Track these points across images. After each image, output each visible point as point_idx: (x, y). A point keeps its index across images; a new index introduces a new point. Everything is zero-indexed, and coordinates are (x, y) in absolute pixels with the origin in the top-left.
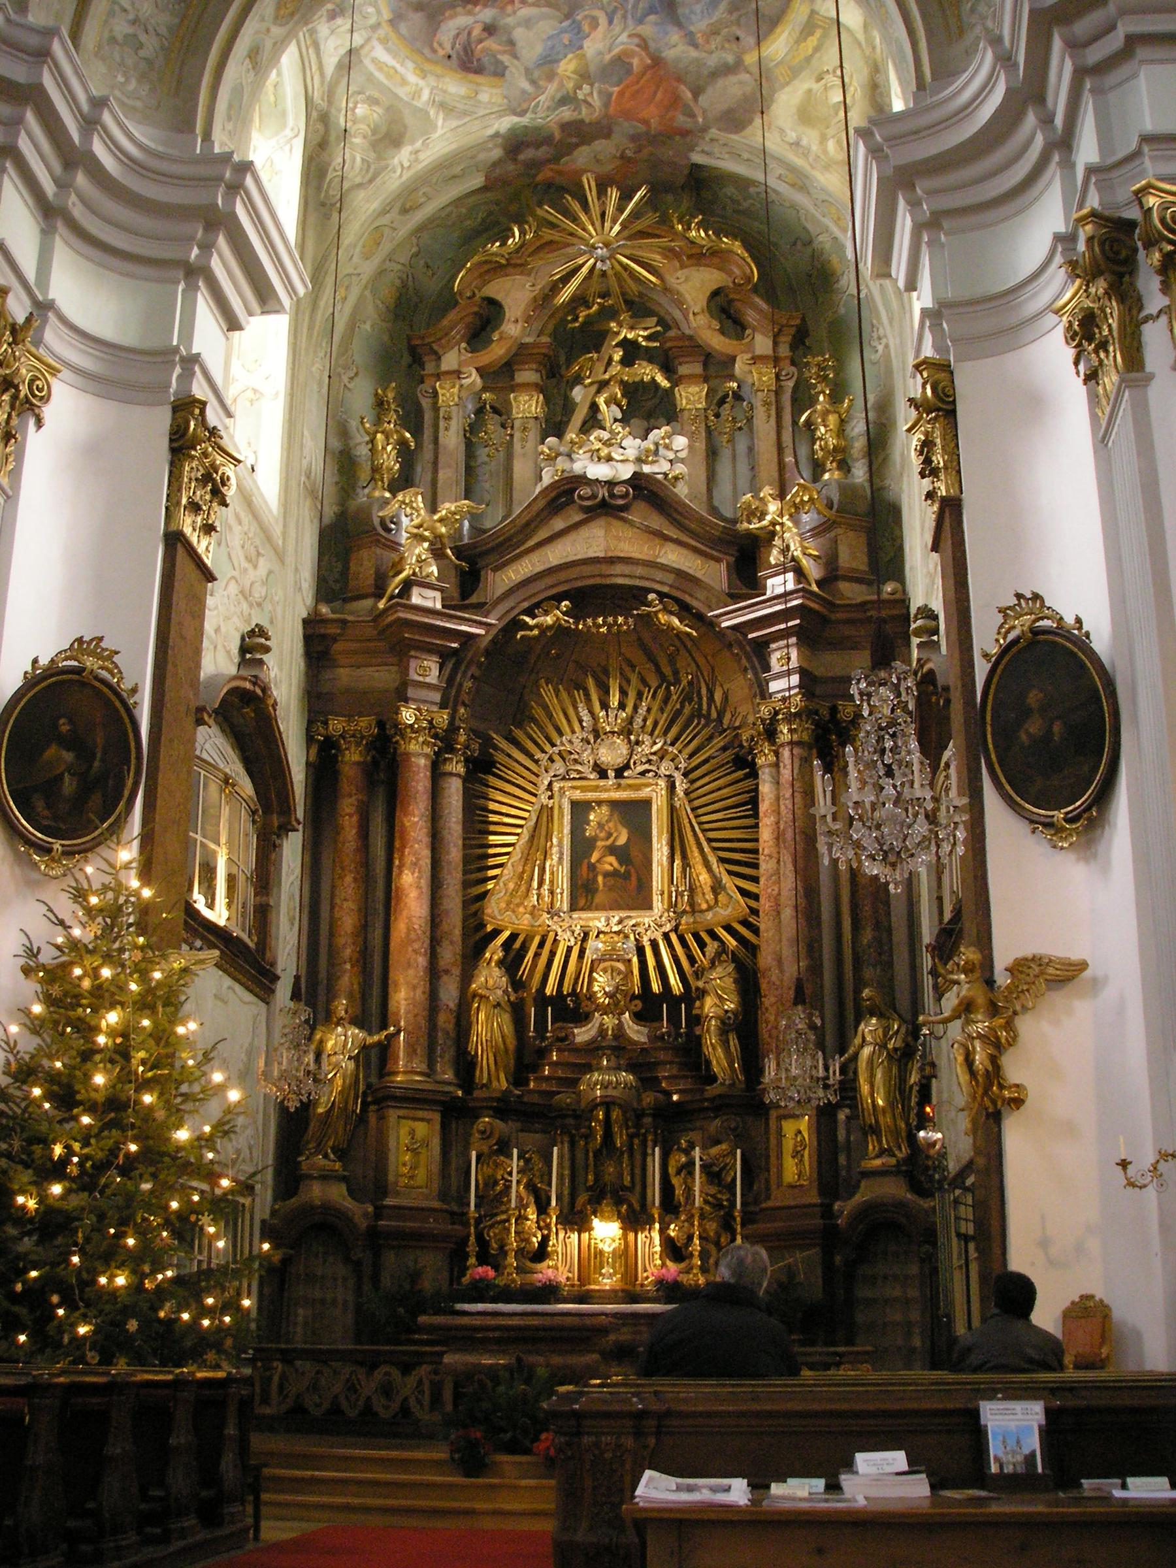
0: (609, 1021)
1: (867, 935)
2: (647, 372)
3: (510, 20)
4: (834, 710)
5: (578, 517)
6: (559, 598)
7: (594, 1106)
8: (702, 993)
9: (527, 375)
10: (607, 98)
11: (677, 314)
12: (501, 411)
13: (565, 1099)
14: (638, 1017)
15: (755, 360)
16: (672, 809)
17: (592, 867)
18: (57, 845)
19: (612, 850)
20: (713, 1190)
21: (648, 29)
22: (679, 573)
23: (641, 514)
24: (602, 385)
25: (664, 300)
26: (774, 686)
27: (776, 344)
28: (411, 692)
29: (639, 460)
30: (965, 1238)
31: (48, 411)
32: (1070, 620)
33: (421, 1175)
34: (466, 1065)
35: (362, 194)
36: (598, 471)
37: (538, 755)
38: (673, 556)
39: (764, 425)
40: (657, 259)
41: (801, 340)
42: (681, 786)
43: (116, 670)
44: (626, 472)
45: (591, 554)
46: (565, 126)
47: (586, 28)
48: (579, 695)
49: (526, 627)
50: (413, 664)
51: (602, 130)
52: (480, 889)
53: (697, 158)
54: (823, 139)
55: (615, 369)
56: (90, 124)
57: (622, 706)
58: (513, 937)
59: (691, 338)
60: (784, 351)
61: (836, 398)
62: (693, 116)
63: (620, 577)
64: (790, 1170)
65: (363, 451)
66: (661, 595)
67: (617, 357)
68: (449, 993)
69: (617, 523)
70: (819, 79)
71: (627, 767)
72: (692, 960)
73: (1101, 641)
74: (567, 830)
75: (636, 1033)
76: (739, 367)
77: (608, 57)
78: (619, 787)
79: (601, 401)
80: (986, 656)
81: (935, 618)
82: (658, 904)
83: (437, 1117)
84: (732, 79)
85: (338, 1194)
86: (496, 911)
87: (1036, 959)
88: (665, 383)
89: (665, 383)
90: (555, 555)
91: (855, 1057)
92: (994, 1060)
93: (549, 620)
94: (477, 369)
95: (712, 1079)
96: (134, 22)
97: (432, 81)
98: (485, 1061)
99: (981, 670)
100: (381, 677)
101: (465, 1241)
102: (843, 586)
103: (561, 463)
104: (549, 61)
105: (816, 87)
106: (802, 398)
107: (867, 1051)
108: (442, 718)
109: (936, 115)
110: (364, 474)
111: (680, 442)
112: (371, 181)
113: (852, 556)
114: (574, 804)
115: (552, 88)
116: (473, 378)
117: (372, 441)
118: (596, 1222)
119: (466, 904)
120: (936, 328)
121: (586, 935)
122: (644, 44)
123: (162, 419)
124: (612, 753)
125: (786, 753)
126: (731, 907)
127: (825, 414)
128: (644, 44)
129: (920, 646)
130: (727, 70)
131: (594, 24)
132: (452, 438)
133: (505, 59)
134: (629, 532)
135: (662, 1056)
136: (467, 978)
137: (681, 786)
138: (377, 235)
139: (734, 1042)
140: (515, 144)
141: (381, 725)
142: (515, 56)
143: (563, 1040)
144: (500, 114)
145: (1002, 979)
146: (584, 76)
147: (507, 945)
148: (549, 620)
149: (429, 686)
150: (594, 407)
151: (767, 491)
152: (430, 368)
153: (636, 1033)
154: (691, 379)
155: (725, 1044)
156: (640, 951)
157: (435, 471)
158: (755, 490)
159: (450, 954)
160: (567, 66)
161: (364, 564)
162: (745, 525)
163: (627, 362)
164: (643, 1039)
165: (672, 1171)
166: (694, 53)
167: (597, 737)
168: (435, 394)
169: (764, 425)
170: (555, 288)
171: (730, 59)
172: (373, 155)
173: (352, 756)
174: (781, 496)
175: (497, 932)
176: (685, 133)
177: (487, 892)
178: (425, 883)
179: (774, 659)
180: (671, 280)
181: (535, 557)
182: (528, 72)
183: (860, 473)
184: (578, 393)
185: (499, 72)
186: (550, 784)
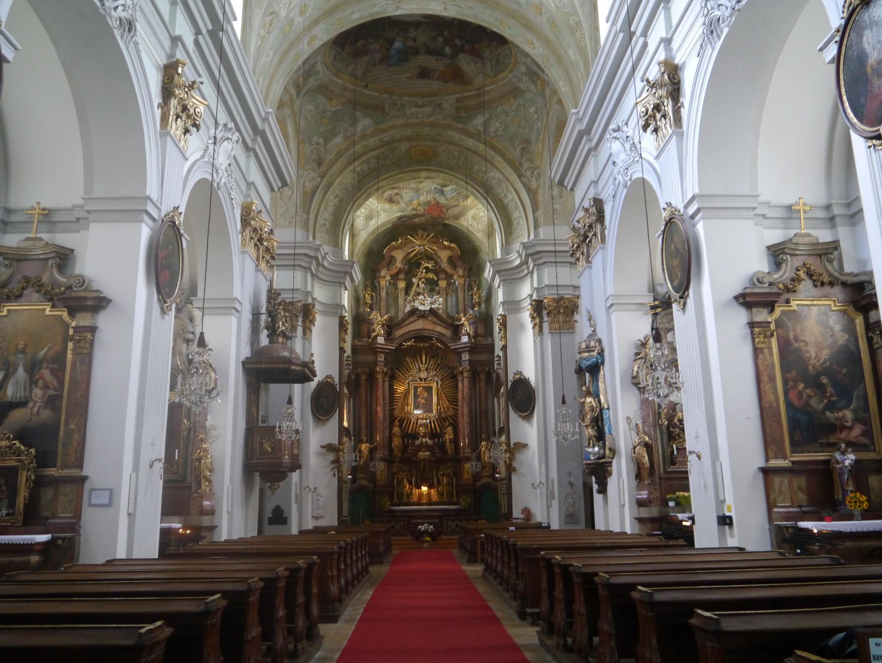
0: (424, 440)
1: (483, 421)
2: (431, 275)
3: (402, 192)
4: (476, 369)
5: (416, 318)
6: (412, 338)
7: (421, 460)
8: (445, 434)
9: (402, 276)
10: (425, 210)
11: (439, 260)
12: (395, 285)
13: (414, 458)
14: (430, 438)
15: (459, 276)
16: (437, 388)
17: (419, 402)
18: (324, 418)
19: (423, 398)
20: (448, 479)
21: (437, 196)
22: (441, 333)
23: (432, 318)
24: (420, 279)
25: (436, 257)
26: (462, 363)
27: (464, 272)
28: (378, 363)
29: (431, 304)
30: (504, 494)
31: (316, 323)
32: (527, 377)
33: (383, 478)
34: (391, 450)
35: (362, 232)
36: (421, 308)
37: (406, 375)
38: (439, 329)
39: (460, 294)
40: (435, 248)
41: (470, 270)
42: (439, 384)
43: (334, 381)
44: (428, 308)
45: (420, 328)
46: (413, 215)
47: (421, 194)
48: (415, 360)
49: (404, 345)
50: (378, 356)
51: (422, 215)
52: (392, 407)
53: (446, 222)
54: (478, 224)
55: (423, 275)
56: (324, 258)
57: (426, 363)
58: (400, 419)
59: (443, 269)
60: (466, 274)
61: (478, 289)
62: (445, 215)
63: (426, 334)
64: (466, 476)
65: (361, 295)
66: (436, 338)
67: (424, 271)
68: (387, 433)
69: (426, 320)
70: (478, 210)
71: (427, 378)
72: (443, 426)
73: (533, 382)
74: (413, 394)
75: (430, 442)
76: (455, 277)
77: (425, 201)
78: (425, 383)
79: (420, 283)
80: (511, 381)
81: (500, 357)
82: (435, 412)
83: (386, 464)
84: (456, 208)
85: (365, 482)
86: (396, 413)
87: (518, 443)
88: (436, 279)
89: (436, 279)
90: (411, 327)
91: (480, 451)
92: (510, 462)
93: (409, 344)
94: (390, 276)
95: (448, 453)
96: (325, 220)
97: (381, 204)
98: (396, 449)
99: (510, 384)
100: (370, 358)
101: (394, 492)
102: (480, 339)
103: (412, 303)
104: (410, 202)
105: (477, 211)
106: (470, 288)
107: (483, 449)
108: (385, 369)
109: (504, 261)
110: (362, 302)
111: (441, 300)
112: (365, 228)
113: (481, 330)
114: (414, 387)
115: (411, 207)
116: (388, 278)
117: (365, 296)
118: (422, 487)
119: (390, 410)
120: (503, 306)
121: (418, 419)
122: (435, 199)
123: (337, 320)
124: (423, 375)
125: (465, 380)
126: (451, 412)
127: (476, 294)
128: (435, 199)
129: (497, 364)
130: (455, 206)
131: (423, 194)
132: (383, 294)
133: (400, 200)
134: (428, 322)
135: (435, 448)
136: (391, 430)
137: (439, 384)
138: (365, 241)
139: (452, 445)
140: (400, 218)
141: (370, 370)
142: (402, 199)
143: (413, 444)
144: (398, 212)
145: (512, 446)
146: (419, 204)
147: (399, 421)
148: (409, 344)
149: (382, 361)
150: (418, 285)
151: (461, 315)
152: (378, 273)
153: (430, 442)
154: (443, 279)
155: (451, 445)
156: (430, 422)
157: (380, 302)
158: (458, 313)
159: (387, 424)
160: (415, 202)
161: (365, 328)
162: (456, 323)
163: (426, 273)
164: (431, 444)
165: (439, 475)
166: (447, 202)
167: (420, 371)
168: (379, 282)
169: (460, 294)
170: (409, 253)
171: (456, 204)
172: (365, 222)
173: (364, 377)
174: (465, 316)
175: (396, 418)
176: (443, 218)
177: (394, 409)
178: (382, 409)
179: (463, 356)
180: (438, 253)
181: (405, 327)
182: (405, 203)
183: (483, 306)
184: (414, 280)
185: (398, 203)
186: (409, 382)
